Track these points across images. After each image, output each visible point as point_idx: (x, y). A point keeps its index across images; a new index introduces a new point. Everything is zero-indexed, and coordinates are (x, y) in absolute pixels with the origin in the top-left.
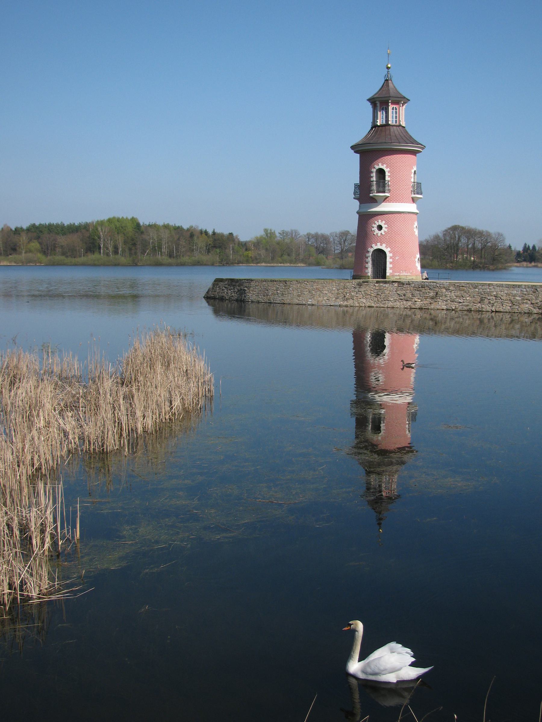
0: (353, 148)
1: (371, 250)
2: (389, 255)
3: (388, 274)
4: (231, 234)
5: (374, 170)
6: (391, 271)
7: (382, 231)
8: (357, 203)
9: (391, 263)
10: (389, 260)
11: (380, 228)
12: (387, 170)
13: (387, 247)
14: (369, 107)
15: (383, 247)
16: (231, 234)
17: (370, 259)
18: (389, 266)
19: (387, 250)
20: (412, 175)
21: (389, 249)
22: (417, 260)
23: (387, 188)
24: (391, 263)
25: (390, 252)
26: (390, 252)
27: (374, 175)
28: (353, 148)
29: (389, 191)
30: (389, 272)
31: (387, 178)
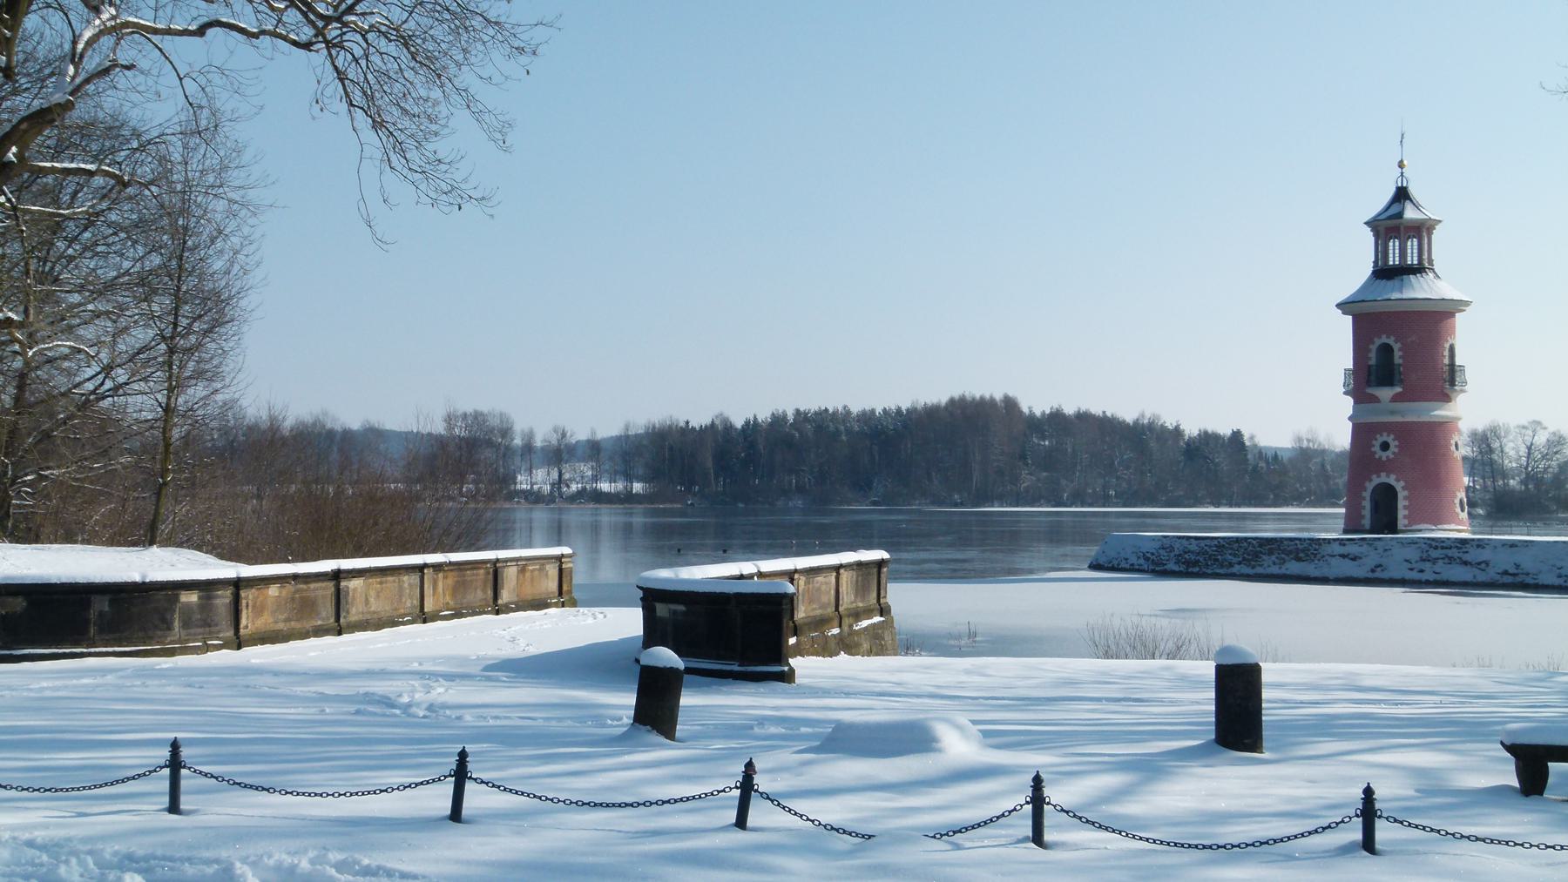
0: (1339, 306)
1: (1370, 486)
2: (1402, 494)
4: (1237, 435)
5: (1374, 348)
7: (1389, 453)
8: (1350, 401)
9: (1405, 507)
10: (1401, 503)
11: (1385, 446)
12: (1396, 347)
13: (1398, 480)
14: (1368, 237)
15: (1392, 480)
16: (1237, 435)
17: (1367, 504)
19: (1399, 486)
20: (1446, 353)
21: (1402, 483)
22: (1457, 501)
23: (1397, 377)
24: (1405, 507)
25: (1404, 488)
26: (1404, 488)
27: (1373, 355)
28: (1339, 306)
29: (1401, 381)
31: (1397, 360)
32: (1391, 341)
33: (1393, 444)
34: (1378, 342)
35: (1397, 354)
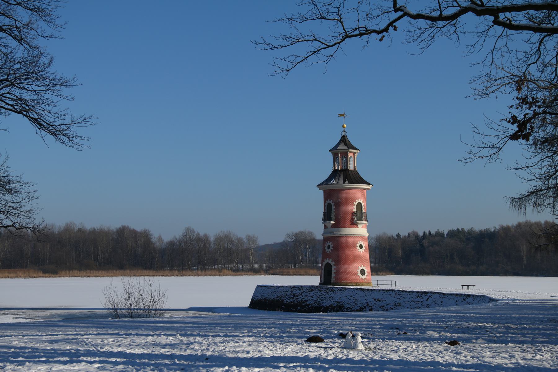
2: (333, 267)
3: (332, 282)
6: (334, 279)
7: (330, 250)
10: (333, 271)
11: (329, 247)
12: (333, 204)
13: (332, 261)
14: (331, 157)
15: (330, 261)
18: (333, 275)
19: (332, 264)
21: (334, 263)
25: (334, 265)
26: (334, 265)
30: (333, 280)
32: (331, 202)
33: (331, 246)
34: (327, 202)
35: (333, 207)
